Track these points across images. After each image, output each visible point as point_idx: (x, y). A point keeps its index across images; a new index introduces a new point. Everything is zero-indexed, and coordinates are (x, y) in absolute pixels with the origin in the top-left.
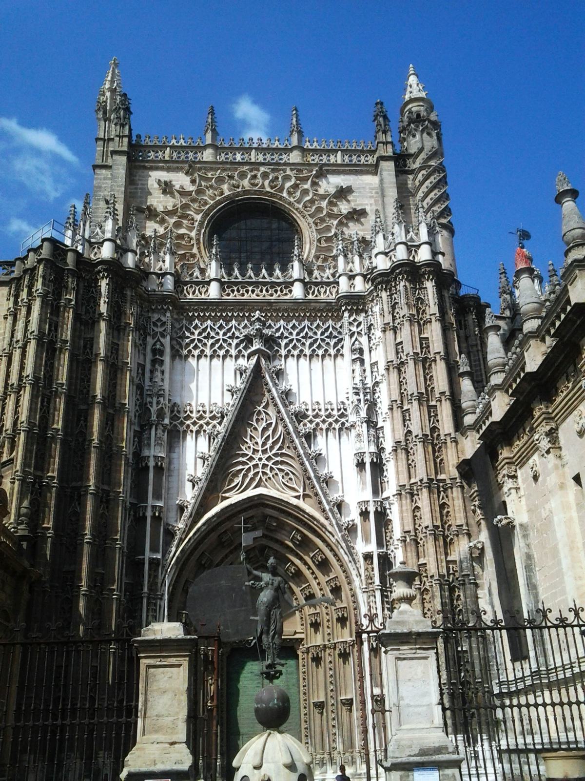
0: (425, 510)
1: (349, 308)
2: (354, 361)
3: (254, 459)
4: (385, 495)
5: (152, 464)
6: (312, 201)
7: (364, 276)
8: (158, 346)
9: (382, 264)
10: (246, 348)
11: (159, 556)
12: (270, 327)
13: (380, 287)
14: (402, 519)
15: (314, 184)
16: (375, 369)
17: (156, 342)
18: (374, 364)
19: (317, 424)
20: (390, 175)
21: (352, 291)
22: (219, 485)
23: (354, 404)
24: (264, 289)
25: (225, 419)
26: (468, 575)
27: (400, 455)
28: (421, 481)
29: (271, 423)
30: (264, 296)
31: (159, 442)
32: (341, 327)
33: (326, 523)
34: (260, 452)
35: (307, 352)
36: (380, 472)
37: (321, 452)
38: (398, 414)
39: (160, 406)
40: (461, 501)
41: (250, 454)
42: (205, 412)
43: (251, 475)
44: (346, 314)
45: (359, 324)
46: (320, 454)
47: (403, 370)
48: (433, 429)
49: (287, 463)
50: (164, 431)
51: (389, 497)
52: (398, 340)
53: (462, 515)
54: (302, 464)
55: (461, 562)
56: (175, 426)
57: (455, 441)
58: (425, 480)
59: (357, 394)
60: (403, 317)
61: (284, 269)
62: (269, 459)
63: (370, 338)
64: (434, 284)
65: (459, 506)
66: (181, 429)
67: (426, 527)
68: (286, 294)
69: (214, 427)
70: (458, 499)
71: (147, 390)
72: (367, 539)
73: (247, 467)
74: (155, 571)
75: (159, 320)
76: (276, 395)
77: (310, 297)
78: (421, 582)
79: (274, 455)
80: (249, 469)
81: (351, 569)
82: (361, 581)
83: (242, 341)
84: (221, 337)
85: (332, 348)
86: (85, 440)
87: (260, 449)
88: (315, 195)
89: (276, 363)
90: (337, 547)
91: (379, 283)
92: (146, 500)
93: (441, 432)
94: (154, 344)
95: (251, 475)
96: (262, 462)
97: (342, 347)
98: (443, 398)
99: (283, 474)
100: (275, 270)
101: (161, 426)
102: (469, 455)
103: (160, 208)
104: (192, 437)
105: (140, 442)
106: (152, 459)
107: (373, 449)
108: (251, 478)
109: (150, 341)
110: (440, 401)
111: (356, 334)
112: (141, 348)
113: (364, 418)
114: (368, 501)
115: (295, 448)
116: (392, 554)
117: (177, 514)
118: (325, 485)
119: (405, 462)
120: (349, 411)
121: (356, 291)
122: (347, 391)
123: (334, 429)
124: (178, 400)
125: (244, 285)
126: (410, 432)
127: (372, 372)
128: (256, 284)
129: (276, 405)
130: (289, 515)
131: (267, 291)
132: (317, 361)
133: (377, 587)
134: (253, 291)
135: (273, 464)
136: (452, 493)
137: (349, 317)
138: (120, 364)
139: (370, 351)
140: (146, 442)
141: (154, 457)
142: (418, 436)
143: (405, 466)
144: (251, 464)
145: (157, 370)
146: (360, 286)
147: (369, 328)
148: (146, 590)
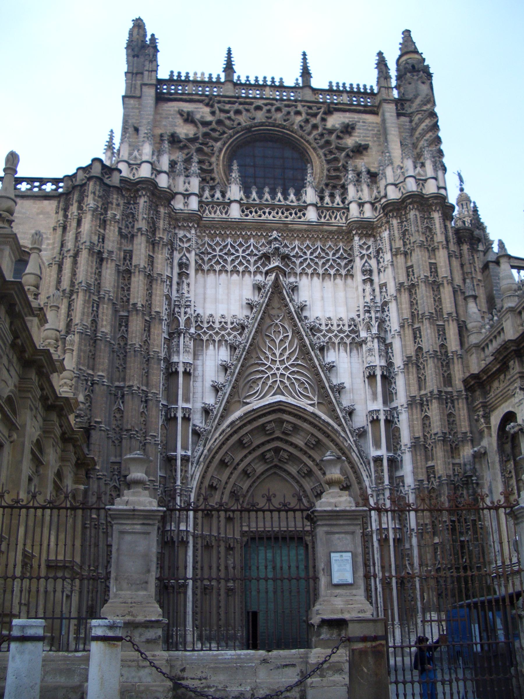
0: (434, 419)
1: (359, 232)
2: (364, 281)
4: (394, 405)
5: (181, 369)
6: (322, 135)
7: (372, 204)
8: (184, 261)
9: (393, 194)
10: (264, 265)
11: (189, 453)
12: (286, 246)
13: (391, 214)
14: (411, 427)
15: (324, 120)
16: (384, 290)
17: (182, 257)
18: (383, 286)
19: (330, 338)
20: (391, 116)
21: (362, 216)
22: (240, 391)
23: (365, 321)
24: (280, 211)
25: (246, 330)
26: (471, 476)
27: (411, 370)
28: (431, 392)
29: (288, 336)
30: (280, 218)
31: (188, 349)
32: (350, 249)
33: (339, 429)
34: (278, 362)
35: (321, 271)
36: (389, 383)
37: (335, 364)
38: (409, 332)
39: (187, 316)
40: (466, 411)
41: (269, 364)
43: (269, 383)
44: (356, 238)
45: (368, 248)
46: (334, 366)
47: (413, 291)
48: (442, 346)
49: (303, 373)
50: (190, 340)
51: (397, 407)
52: (409, 264)
53: (467, 423)
54: (318, 374)
55: (465, 465)
56: (199, 335)
57: (461, 357)
58: (436, 392)
59: (369, 312)
60: (414, 243)
61: (298, 194)
62: (286, 368)
63: (378, 262)
64: (440, 215)
65: (464, 416)
66: (205, 338)
67: (436, 434)
68: (287, 217)
69: (235, 337)
70: (463, 410)
71: (175, 301)
72: (377, 445)
73: (267, 375)
74: (185, 466)
75: (185, 236)
76: (293, 310)
77: (323, 220)
78: (429, 482)
79: (290, 365)
80: (268, 376)
81: (362, 470)
82: (371, 481)
83: (260, 258)
84: (241, 254)
85: (343, 268)
86: (126, 344)
87: (278, 359)
88: (324, 129)
89: (292, 279)
90: (349, 451)
91: (391, 211)
92: (176, 402)
93: (449, 349)
94: (181, 259)
95: (269, 383)
96: (280, 372)
97: (352, 268)
98: (450, 319)
100: (289, 195)
102: (475, 369)
103: (182, 136)
104: (214, 346)
105: (169, 348)
108: (270, 386)
109: (177, 256)
110: (448, 321)
111: (366, 257)
113: (375, 334)
114: (379, 411)
115: (311, 359)
116: (399, 459)
117: (202, 416)
119: (415, 375)
121: (365, 216)
122: (357, 309)
123: (345, 343)
124: (200, 311)
125: (261, 207)
126: (420, 349)
127: (381, 292)
128: (273, 207)
129: (293, 319)
130: (305, 420)
131: (283, 213)
132: (328, 280)
134: (270, 213)
136: (458, 404)
137: (359, 240)
138: (155, 275)
139: (379, 273)
140: (175, 349)
141: (183, 363)
142: (428, 351)
143: (416, 379)
144: (269, 374)
145: (183, 282)
146: (368, 212)
147: (378, 252)
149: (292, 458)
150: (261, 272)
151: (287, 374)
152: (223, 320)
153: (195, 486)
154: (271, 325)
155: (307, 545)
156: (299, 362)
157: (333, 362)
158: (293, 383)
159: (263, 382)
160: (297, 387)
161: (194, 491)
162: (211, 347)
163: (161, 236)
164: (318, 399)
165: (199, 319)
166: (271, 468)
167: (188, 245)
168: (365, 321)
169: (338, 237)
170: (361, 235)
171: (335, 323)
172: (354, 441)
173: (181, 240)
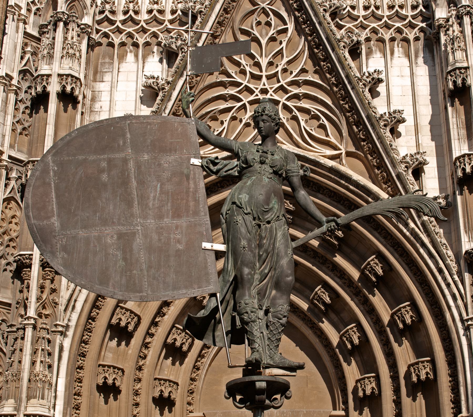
3: (251, 92)
25: (199, 19)
34: (264, 79)
37: (383, 76)
42: (161, 12)
66: (117, 40)
99: (308, 117)
101: (74, 25)
104: (136, 56)
106: (54, 80)
118: (388, 134)
135: (288, 99)
140: (45, 52)
141: (59, 75)
144: (245, 101)
148: (32, 312)
151: (283, 100)
152: (156, 7)
153: (73, 323)
154: (252, 12)
156: (310, 77)
157: (379, 72)
158: (295, 118)
159: (234, 118)
160: (303, 123)
161: (70, 333)
162: (130, 57)
164: (346, 147)
165: (108, 7)
172: (423, 224)
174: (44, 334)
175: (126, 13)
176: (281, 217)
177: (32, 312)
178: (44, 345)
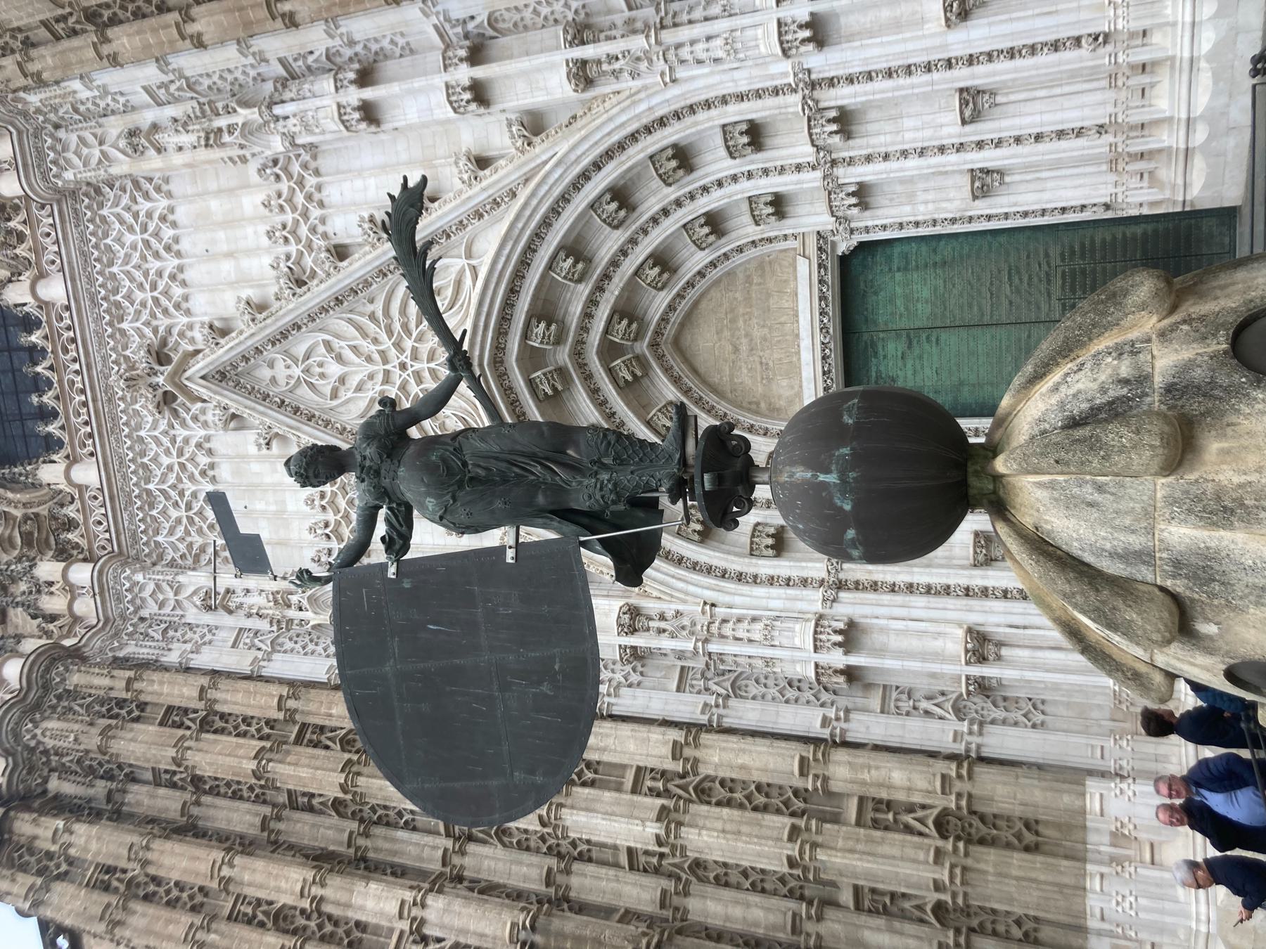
39: (305, 603)
52: (43, 33)
61: (30, 324)
75: (153, 595)
83: (175, 413)
89: (197, 334)
97: (150, 180)
107: (327, 84)
112: (208, 637)
120: (268, 153)
133: (653, 40)
149: (626, 311)
150: (203, 411)
154: (311, 386)
155: (862, 245)
157: (362, 219)
163: (123, 684)
166: (660, 358)
167: (168, 589)
168: (243, 142)
169: (92, 221)
170: (62, 162)
171: (278, 219)
173: (161, 605)
174: (714, 628)
175: (328, 537)
176: (457, 444)
177: (689, 646)
178: (727, 630)
